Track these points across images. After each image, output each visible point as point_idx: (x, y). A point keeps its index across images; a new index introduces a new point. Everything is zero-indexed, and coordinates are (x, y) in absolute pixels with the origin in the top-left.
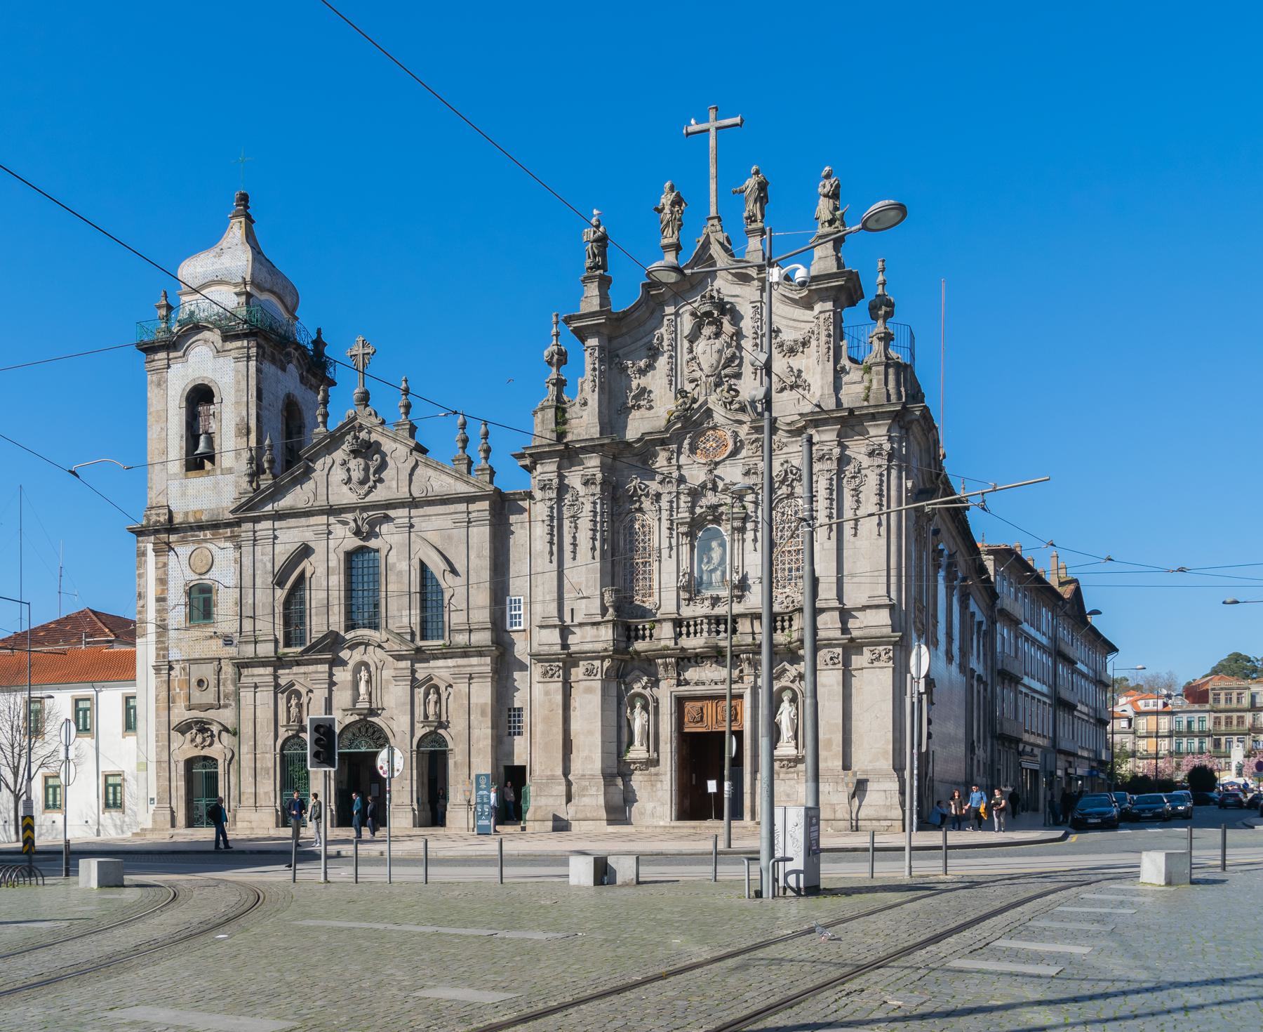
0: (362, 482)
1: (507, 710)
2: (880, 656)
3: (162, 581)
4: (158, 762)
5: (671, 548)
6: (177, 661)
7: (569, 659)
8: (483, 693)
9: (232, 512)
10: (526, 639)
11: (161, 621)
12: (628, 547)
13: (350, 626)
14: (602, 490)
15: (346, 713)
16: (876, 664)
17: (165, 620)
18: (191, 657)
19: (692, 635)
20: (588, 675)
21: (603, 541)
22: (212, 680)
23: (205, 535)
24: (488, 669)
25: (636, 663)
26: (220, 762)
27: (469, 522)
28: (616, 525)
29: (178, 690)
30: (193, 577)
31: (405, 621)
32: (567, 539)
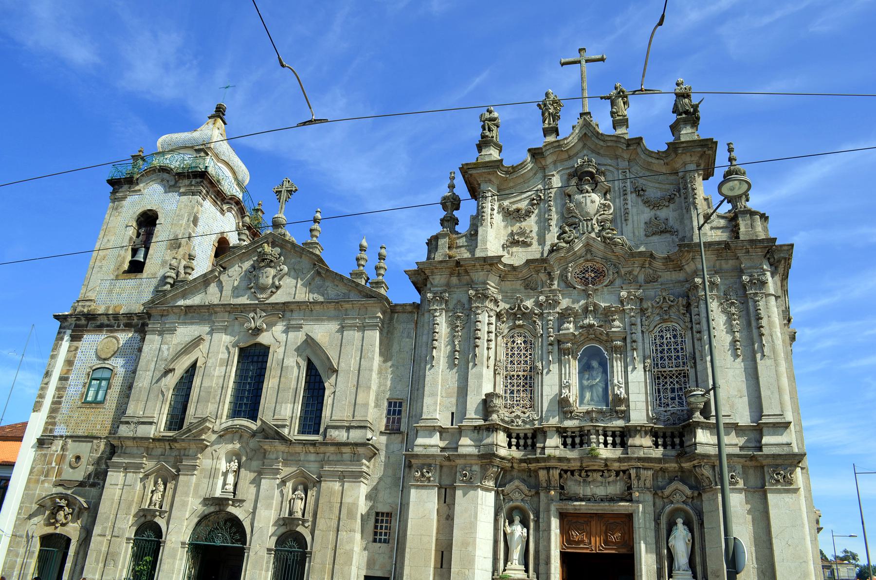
1: (374, 514)
3: (69, 363)
4: (14, 535)
6: (62, 436)
7: (447, 463)
10: (402, 442)
11: (58, 397)
12: (510, 359)
15: (207, 503)
17: (62, 397)
18: (75, 434)
19: (577, 446)
23: (119, 326)
25: (515, 473)
26: (72, 541)
29: (54, 464)
30: (98, 364)
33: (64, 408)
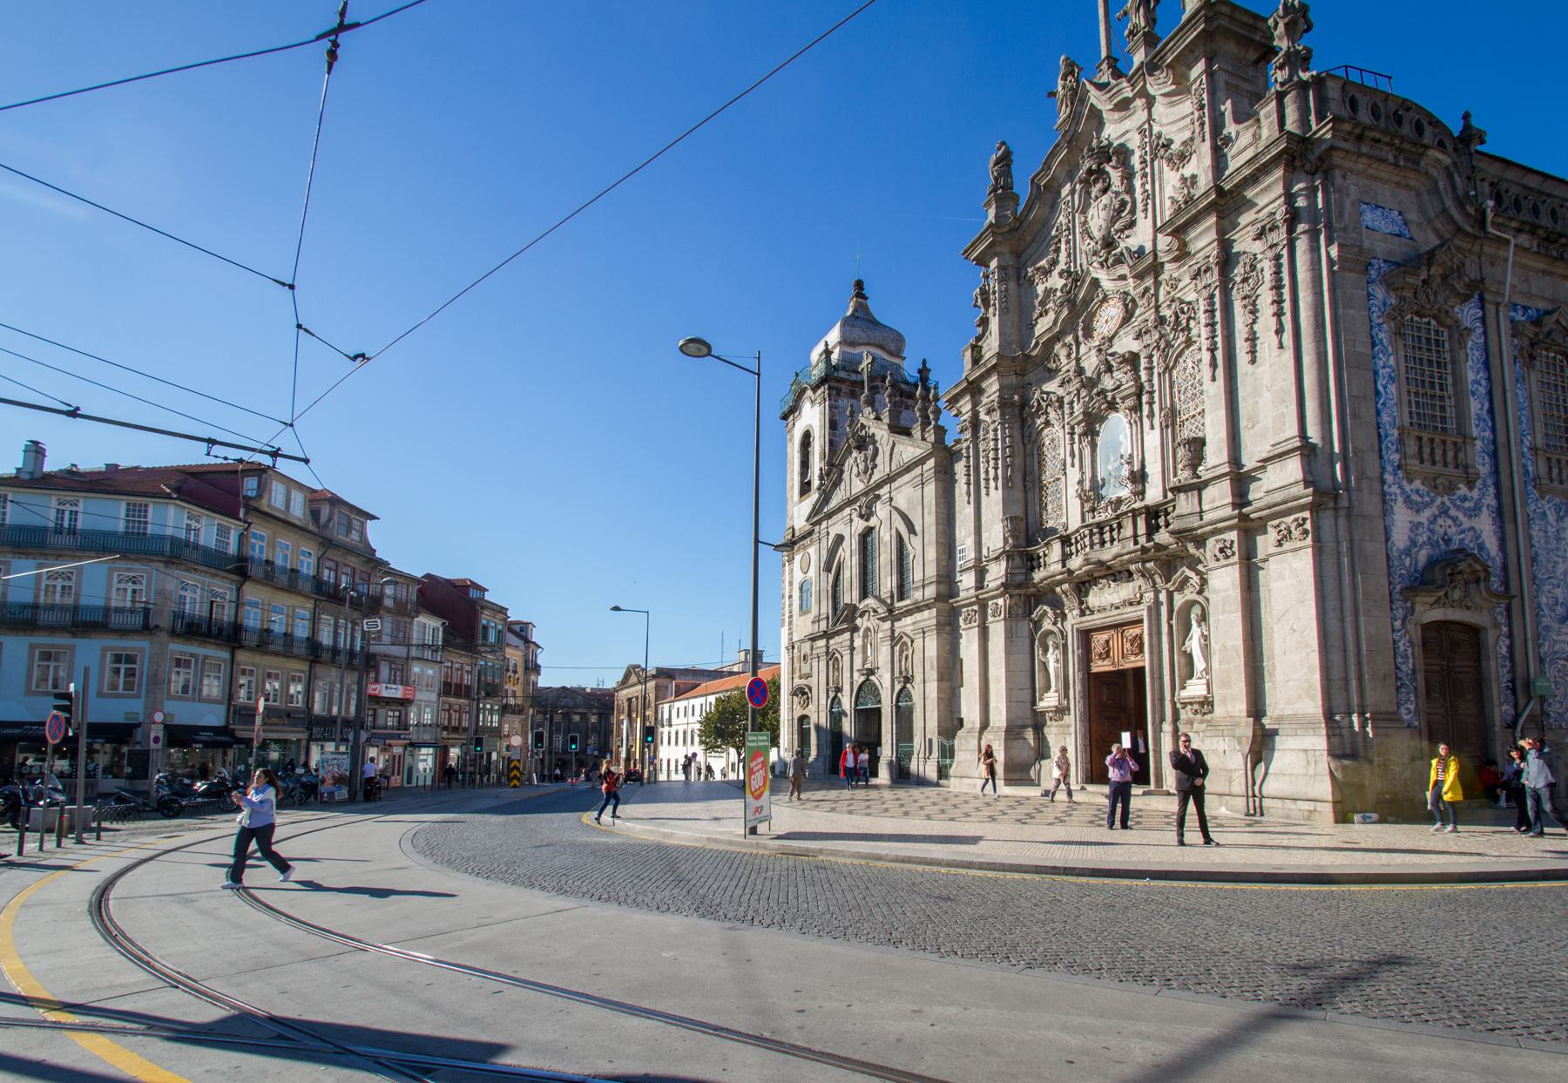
0: (865, 473)
2: (1290, 532)
3: (791, 583)
5: (1073, 455)
8: (931, 646)
9: (807, 520)
13: (864, 594)
14: (1002, 415)
16: (1287, 545)
20: (994, 616)
21: (1005, 467)
22: (809, 653)
24: (934, 621)
27: (923, 484)
28: (1029, 446)
31: (889, 586)
32: (983, 476)
33: (794, 618)
